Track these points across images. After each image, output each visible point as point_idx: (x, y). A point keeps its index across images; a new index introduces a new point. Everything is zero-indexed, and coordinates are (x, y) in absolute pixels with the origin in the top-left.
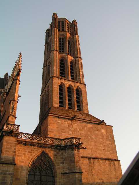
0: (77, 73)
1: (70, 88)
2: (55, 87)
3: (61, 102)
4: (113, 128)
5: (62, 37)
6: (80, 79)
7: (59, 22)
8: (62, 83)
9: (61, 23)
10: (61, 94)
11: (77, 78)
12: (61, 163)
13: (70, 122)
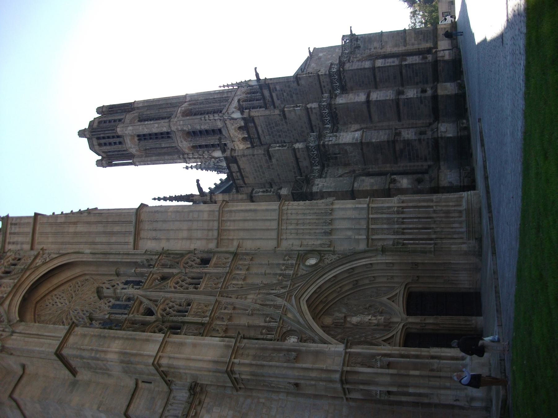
0: (216, 97)
4: (317, 47)
11: (225, 97)
12: (370, 50)
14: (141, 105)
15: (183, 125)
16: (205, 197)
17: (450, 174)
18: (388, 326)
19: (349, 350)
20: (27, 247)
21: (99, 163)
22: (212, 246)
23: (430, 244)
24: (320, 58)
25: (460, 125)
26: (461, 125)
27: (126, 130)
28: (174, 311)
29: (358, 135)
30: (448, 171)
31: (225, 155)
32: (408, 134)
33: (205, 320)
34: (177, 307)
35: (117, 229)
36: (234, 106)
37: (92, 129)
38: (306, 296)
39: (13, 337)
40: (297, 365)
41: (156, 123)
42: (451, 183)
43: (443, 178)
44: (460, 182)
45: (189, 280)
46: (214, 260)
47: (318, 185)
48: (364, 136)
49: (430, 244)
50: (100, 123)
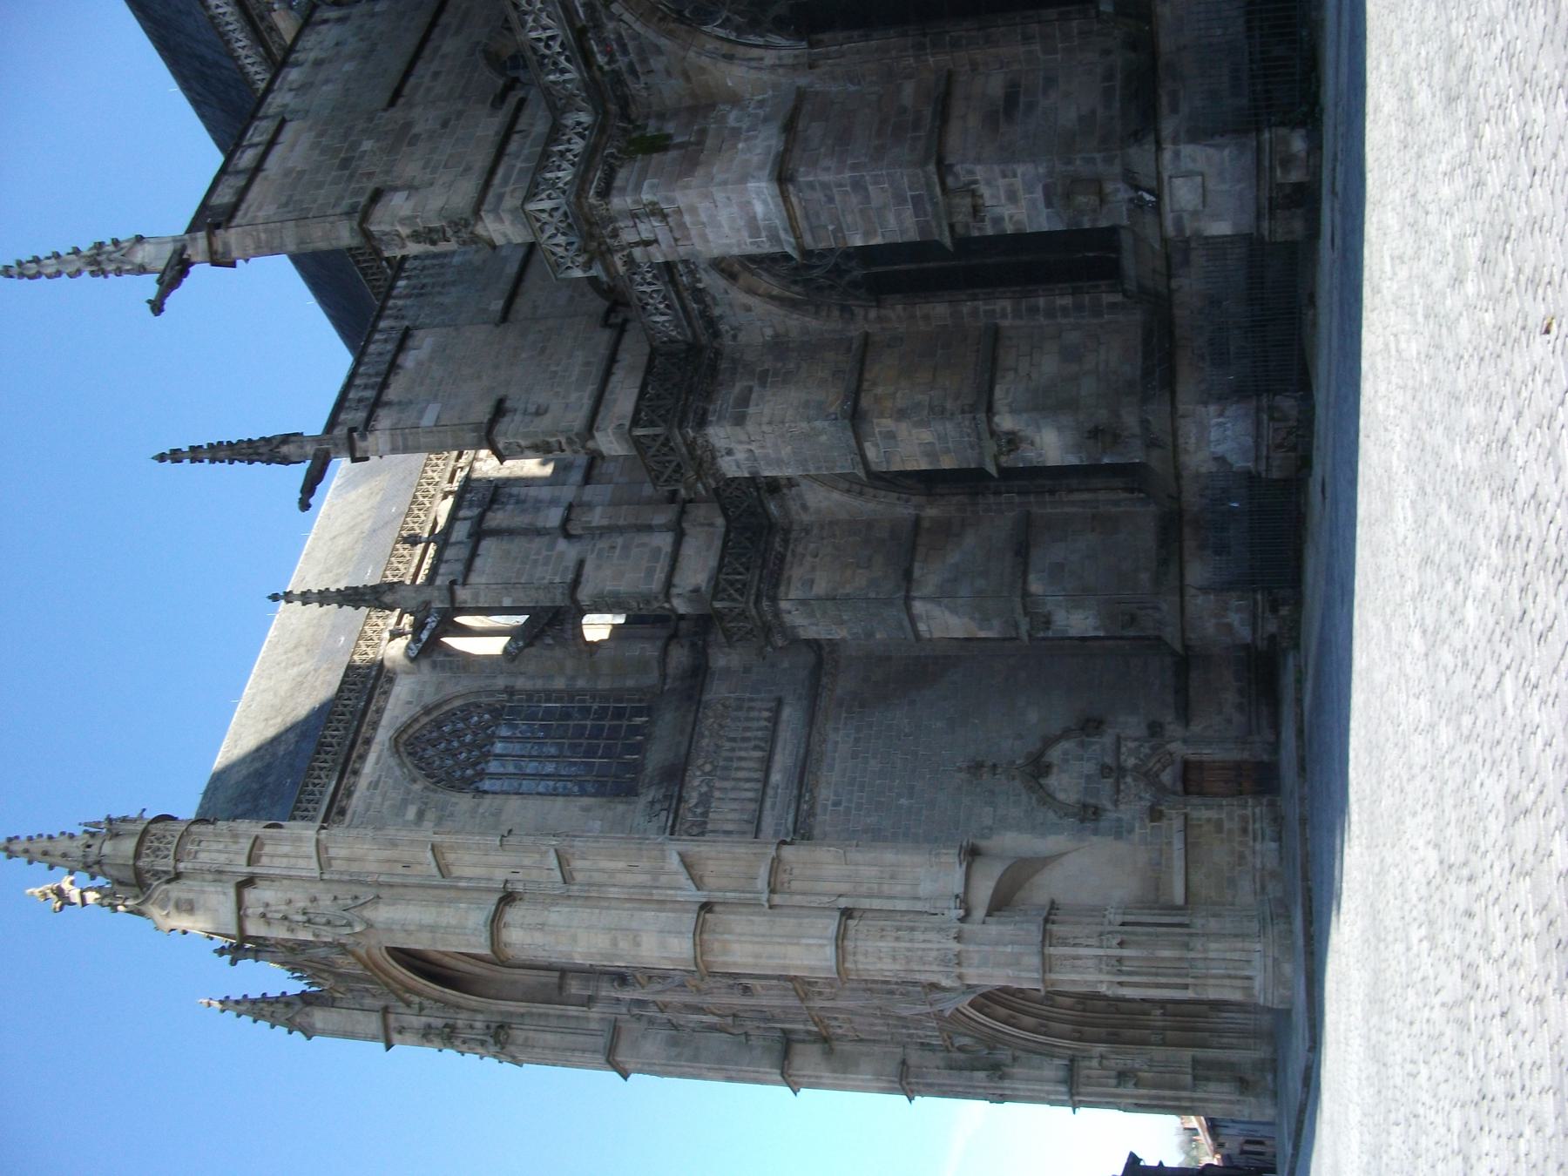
17: (1219, 425)
25: (1272, 168)
26: (1279, 172)
29: (765, 202)
30: (1213, 409)
32: (1012, 197)
42: (1220, 460)
43: (1193, 440)
44: (1257, 459)
47: (730, 452)
48: (799, 213)
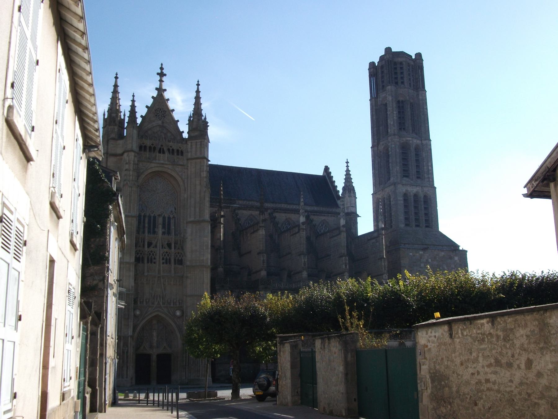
0: (425, 168)
1: (416, 196)
2: (399, 200)
3: (406, 219)
4: (467, 253)
5: (401, 99)
6: (429, 179)
7: (395, 63)
8: (407, 191)
9: (398, 66)
10: (406, 206)
13: (421, 252)
14: (420, 97)
15: (391, 148)
16: (261, 223)
18: (151, 347)
19: (129, 338)
20: (189, 156)
21: (372, 64)
22: (188, 263)
23: (186, 363)
24: (451, 258)
27: (389, 94)
28: (151, 256)
31: (301, 225)
33: (146, 274)
34: (153, 257)
35: (197, 209)
36: (409, 189)
37: (391, 61)
38: (160, 314)
39: (129, 188)
40: (123, 319)
41: (394, 122)
45: (168, 258)
46: (180, 266)
49: (186, 363)
50: (401, 63)
